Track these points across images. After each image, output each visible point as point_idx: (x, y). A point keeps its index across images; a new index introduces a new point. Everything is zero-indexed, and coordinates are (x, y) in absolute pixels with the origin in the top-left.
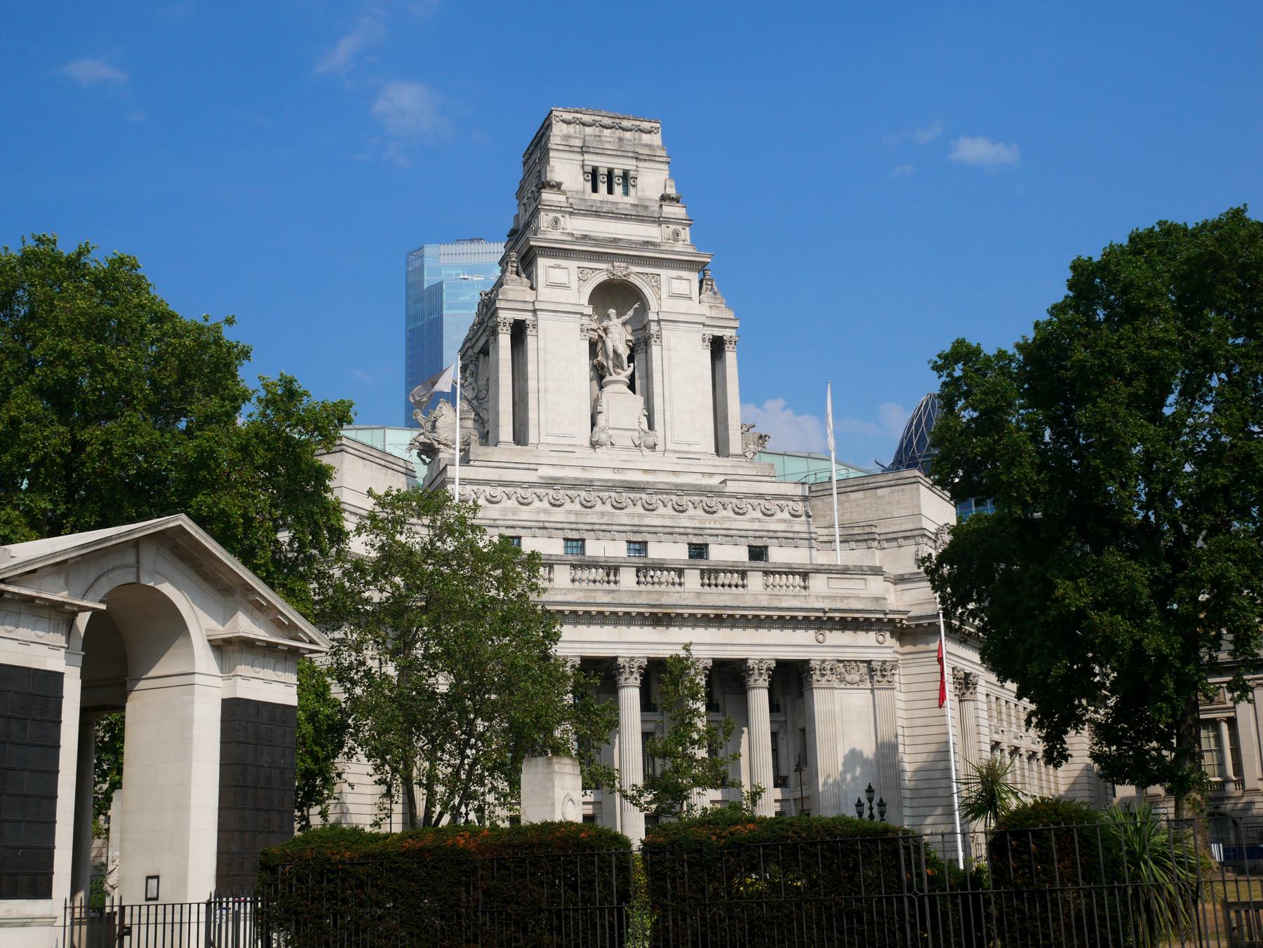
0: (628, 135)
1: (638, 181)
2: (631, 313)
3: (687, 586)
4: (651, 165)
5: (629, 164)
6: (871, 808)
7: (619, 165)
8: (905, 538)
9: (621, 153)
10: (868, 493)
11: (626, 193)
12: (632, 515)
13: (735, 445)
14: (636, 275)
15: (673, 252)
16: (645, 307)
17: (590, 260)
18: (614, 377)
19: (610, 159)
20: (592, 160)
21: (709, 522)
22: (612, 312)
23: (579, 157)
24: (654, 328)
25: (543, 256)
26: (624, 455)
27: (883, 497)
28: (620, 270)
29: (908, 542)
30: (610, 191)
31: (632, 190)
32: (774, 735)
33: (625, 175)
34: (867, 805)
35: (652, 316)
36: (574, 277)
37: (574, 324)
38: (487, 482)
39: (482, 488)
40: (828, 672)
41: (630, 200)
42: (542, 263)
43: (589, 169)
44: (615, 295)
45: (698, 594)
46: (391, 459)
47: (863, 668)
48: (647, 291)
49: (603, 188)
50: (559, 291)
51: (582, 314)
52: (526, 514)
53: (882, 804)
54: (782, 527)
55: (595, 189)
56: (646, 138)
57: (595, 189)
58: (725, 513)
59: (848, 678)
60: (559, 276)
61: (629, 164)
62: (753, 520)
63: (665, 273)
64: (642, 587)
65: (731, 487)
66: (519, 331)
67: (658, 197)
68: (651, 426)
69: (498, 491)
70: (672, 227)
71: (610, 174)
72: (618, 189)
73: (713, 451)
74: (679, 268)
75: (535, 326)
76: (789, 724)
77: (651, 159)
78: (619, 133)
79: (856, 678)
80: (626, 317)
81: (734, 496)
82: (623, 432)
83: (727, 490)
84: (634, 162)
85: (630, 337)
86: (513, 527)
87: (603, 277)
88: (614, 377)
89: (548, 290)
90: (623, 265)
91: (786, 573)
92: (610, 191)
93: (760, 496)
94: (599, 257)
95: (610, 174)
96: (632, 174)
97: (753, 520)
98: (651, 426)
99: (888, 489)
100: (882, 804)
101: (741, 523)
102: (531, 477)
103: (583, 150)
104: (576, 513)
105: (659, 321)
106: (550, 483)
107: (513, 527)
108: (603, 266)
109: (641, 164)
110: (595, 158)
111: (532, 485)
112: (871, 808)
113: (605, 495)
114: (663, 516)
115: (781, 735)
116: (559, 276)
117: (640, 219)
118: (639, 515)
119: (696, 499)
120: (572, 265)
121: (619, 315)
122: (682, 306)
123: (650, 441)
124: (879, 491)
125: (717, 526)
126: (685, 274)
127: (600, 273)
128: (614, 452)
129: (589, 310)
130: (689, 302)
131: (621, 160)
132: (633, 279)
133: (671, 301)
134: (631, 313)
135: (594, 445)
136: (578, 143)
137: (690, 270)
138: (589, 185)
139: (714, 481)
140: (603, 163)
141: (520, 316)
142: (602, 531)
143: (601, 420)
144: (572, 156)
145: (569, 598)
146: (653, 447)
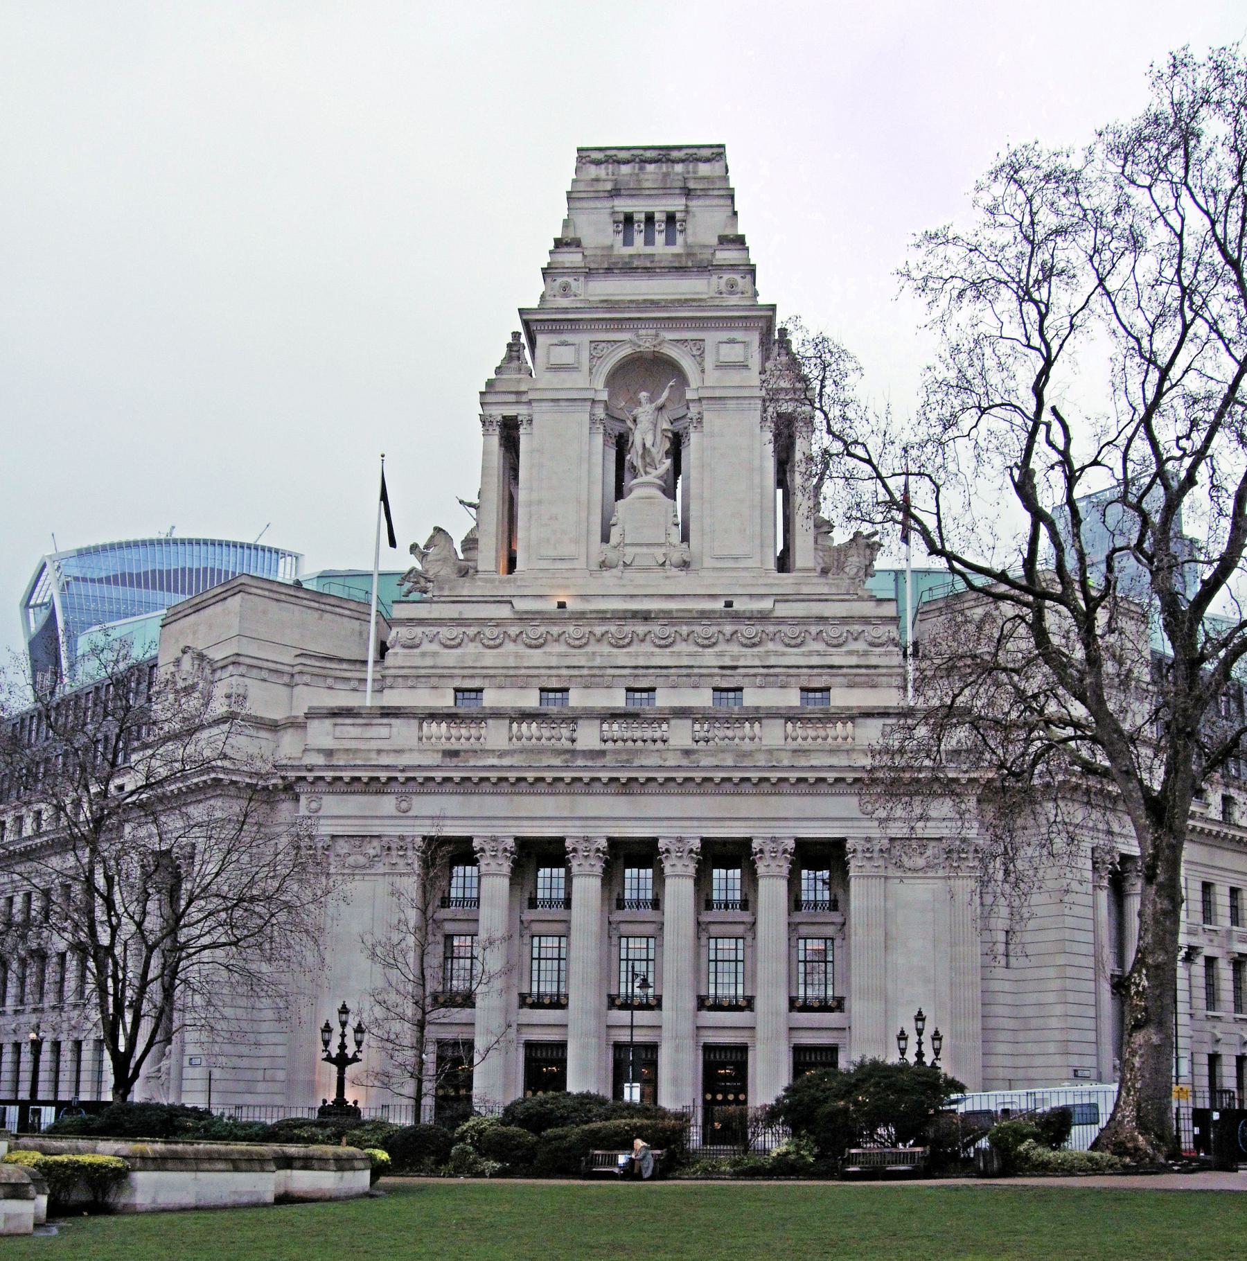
0: (679, 168)
1: (690, 220)
2: (665, 394)
3: (671, 742)
4: (708, 202)
5: (676, 204)
6: (920, 1043)
7: (660, 208)
9: (665, 191)
11: (670, 241)
12: (637, 655)
13: (804, 555)
14: (671, 345)
15: (727, 308)
16: (683, 380)
17: (607, 330)
18: (644, 479)
19: (650, 202)
20: (624, 205)
21: (749, 658)
23: (608, 204)
24: (693, 411)
25: (542, 332)
26: (640, 578)
28: (645, 340)
30: (649, 241)
31: (680, 239)
33: (671, 219)
34: (913, 1038)
35: (690, 395)
36: (585, 356)
37: (582, 416)
38: (439, 622)
39: (435, 630)
40: (875, 855)
41: (677, 249)
42: (541, 340)
43: (622, 218)
44: (648, 370)
45: (687, 753)
46: (332, 601)
48: (688, 365)
49: (639, 239)
50: (563, 375)
51: (593, 401)
52: (490, 658)
53: (937, 1037)
54: (854, 661)
55: (628, 242)
56: (704, 169)
57: (628, 242)
58: (771, 646)
59: (907, 862)
60: (565, 355)
61: (676, 204)
62: (810, 654)
63: (711, 337)
64: (610, 745)
65: (782, 610)
66: (509, 432)
67: (715, 241)
68: (685, 538)
69: (457, 631)
70: (726, 277)
71: (650, 219)
72: (660, 238)
74: (731, 329)
75: (530, 422)
77: (705, 193)
78: (664, 168)
79: (921, 862)
80: (660, 401)
81: (781, 621)
82: (644, 550)
83: (778, 613)
84: (683, 201)
85: (666, 426)
86: (472, 677)
87: (626, 351)
88: (644, 479)
90: (653, 332)
91: (788, 719)
92: (649, 241)
93: (821, 619)
94: (619, 324)
95: (650, 219)
96: (679, 216)
97: (810, 654)
98: (685, 538)
100: (937, 1037)
101: (794, 657)
102: (504, 612)
103: (615, 193)
104: (560, 655)
106: (524, 618)
107: (472, 677)
109: (693, 203)
110: (629, 202)
111: (499, 623)
112: (920, 1043)
113: (598, 630)
114: (679, 654)
116: (565, 355)
117: (679, 269)
118: (645, 654)
119: (728, 629)
120: (583, 339)
121: (651, 400)
122: (735, 378)
123: (676, 557)
125: (757, 663)
126: (739, 335)
127: (625, 344)
128: (628, 574)
129: (604, 396)
130: (745, 373)
131: (664, 202)
133: (718, 373)
134: (665, 394)
135: (603, 565)
136: (609, 186)
137: (746, 329)
138: (621, 235)
139: (767, 604)
140: (638, 207)
141: (510, 411)
142: (593, 680)
143: (614, 539)
144: (598, 204)
145: (506, 762)
146: (685, 565)
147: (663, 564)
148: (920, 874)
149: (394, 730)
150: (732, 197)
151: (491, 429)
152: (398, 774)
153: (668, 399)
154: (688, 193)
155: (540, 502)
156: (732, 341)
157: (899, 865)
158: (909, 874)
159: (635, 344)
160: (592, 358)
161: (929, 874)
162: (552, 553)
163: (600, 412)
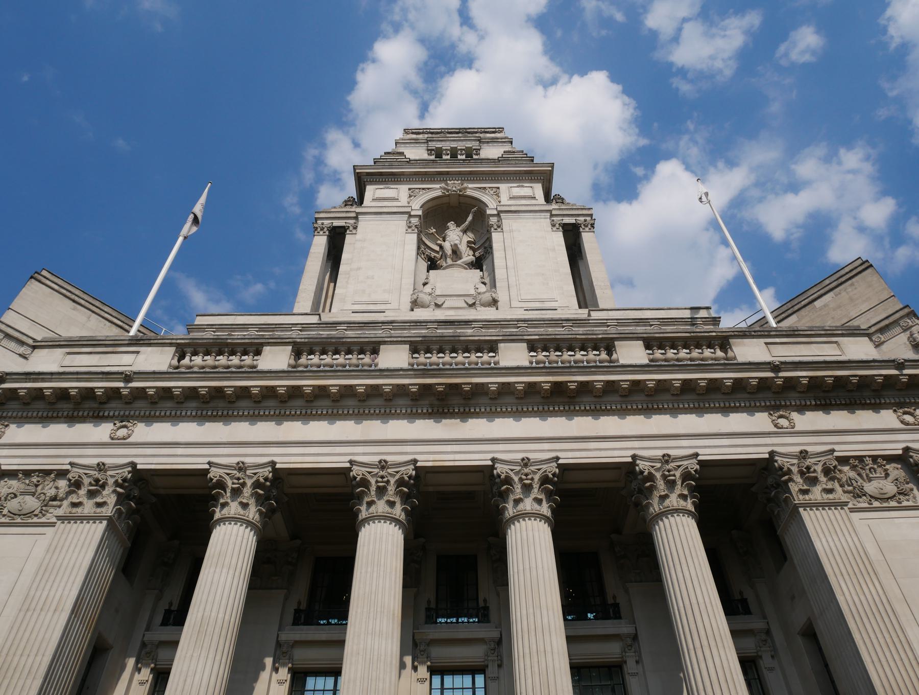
2: (470, 218)
5: (474, 145)
8: (882, 330)
10: (803, 312)
14: (472, 189)
17: (423, 182)
22: (451, 224)
24: (493, 220)
25: (372, 183)
27: (825, 306)
28: (454, 185)
29: (889, 334)
32: (748, 665)
47: (896, 471)
48: (485, 198)
51: (410, 216)
59: (870, 488)
73: (577, 307)
74: (520, 180)
75: (355, 228)
76: (778, 636)
79: (889, 488)
89: (374, 204)
99: (831, 294)
105: (498, 215)
108: (438, 186)
115: (766, 662)
124: (818, 304)
132: (469, 193)
134: (470, 218)
146: (494, 303)
147: (474, 304)
148: (893, 504)
149: (141, 357)
150: (511, 143)
151: (321, 233)
152: (121, 385)
153: (471, 223)
154: (480, 140)
155: (359, 269)
156: (523, 186)
157: (859, 494)
158: (876, 504)
159: (445, 189)
160: (410, 196)
161: (905, 503)
162: (365, 299)
163: (415, 221)
